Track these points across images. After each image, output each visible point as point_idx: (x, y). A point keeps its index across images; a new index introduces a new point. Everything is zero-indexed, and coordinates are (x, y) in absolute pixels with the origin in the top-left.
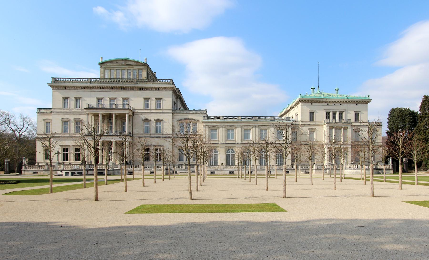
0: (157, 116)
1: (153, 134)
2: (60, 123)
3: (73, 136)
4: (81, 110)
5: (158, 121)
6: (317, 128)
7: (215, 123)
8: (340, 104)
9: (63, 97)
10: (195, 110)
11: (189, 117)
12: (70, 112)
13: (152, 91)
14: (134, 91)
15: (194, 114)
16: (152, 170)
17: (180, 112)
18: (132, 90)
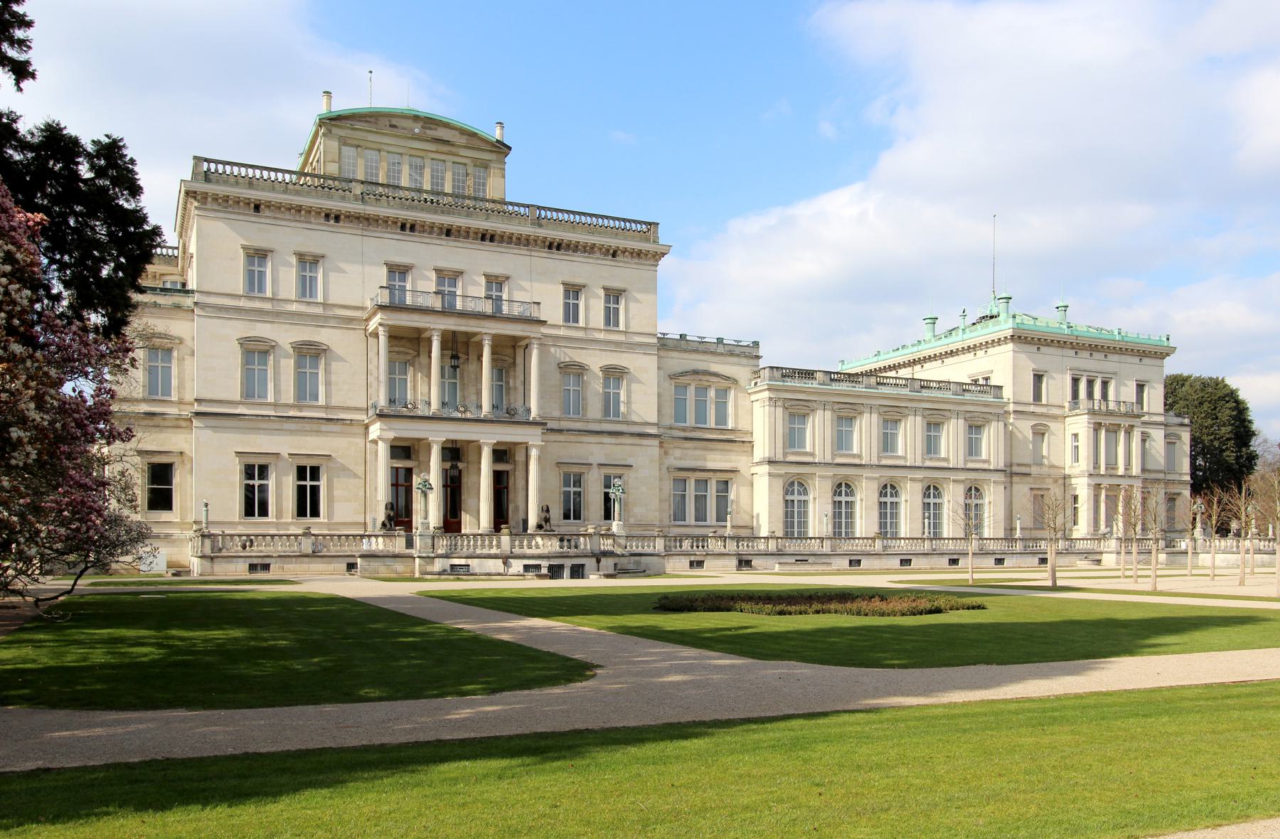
0: (608, 353)
1: (595, 421)
2: (234, 359)
3: (291, 413)
4: (322, 308)
5: (614, 374)
6: (1053, 425)
7: (804, 392)
9: (244, 248)
10: (725, 342)
11: (712, 365)
12: (278, 314)
13: (591, 261)
14: (528, 253)
15: (722, 358)
16: (696, 555)
17: (676, 347)
18: (520, 249)
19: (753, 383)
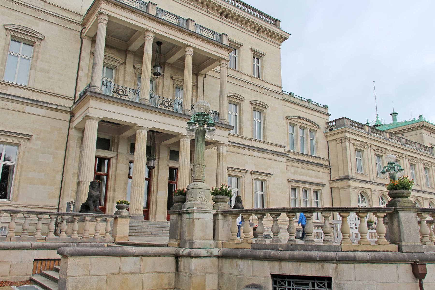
1: (248, 139)
19: (328, 130)
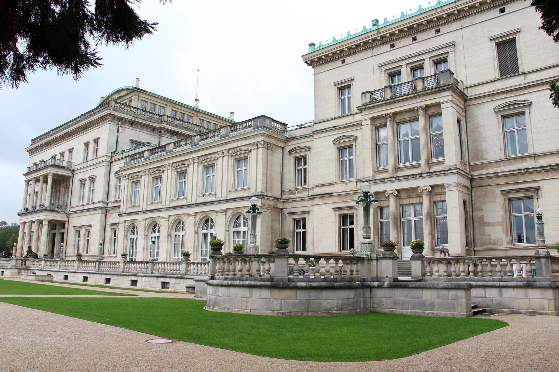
8: (433, 31)
